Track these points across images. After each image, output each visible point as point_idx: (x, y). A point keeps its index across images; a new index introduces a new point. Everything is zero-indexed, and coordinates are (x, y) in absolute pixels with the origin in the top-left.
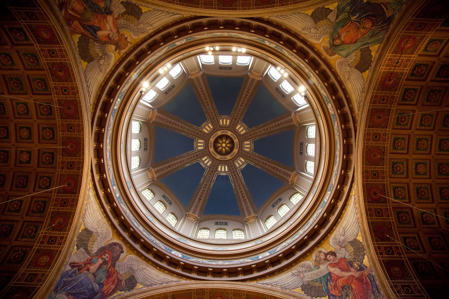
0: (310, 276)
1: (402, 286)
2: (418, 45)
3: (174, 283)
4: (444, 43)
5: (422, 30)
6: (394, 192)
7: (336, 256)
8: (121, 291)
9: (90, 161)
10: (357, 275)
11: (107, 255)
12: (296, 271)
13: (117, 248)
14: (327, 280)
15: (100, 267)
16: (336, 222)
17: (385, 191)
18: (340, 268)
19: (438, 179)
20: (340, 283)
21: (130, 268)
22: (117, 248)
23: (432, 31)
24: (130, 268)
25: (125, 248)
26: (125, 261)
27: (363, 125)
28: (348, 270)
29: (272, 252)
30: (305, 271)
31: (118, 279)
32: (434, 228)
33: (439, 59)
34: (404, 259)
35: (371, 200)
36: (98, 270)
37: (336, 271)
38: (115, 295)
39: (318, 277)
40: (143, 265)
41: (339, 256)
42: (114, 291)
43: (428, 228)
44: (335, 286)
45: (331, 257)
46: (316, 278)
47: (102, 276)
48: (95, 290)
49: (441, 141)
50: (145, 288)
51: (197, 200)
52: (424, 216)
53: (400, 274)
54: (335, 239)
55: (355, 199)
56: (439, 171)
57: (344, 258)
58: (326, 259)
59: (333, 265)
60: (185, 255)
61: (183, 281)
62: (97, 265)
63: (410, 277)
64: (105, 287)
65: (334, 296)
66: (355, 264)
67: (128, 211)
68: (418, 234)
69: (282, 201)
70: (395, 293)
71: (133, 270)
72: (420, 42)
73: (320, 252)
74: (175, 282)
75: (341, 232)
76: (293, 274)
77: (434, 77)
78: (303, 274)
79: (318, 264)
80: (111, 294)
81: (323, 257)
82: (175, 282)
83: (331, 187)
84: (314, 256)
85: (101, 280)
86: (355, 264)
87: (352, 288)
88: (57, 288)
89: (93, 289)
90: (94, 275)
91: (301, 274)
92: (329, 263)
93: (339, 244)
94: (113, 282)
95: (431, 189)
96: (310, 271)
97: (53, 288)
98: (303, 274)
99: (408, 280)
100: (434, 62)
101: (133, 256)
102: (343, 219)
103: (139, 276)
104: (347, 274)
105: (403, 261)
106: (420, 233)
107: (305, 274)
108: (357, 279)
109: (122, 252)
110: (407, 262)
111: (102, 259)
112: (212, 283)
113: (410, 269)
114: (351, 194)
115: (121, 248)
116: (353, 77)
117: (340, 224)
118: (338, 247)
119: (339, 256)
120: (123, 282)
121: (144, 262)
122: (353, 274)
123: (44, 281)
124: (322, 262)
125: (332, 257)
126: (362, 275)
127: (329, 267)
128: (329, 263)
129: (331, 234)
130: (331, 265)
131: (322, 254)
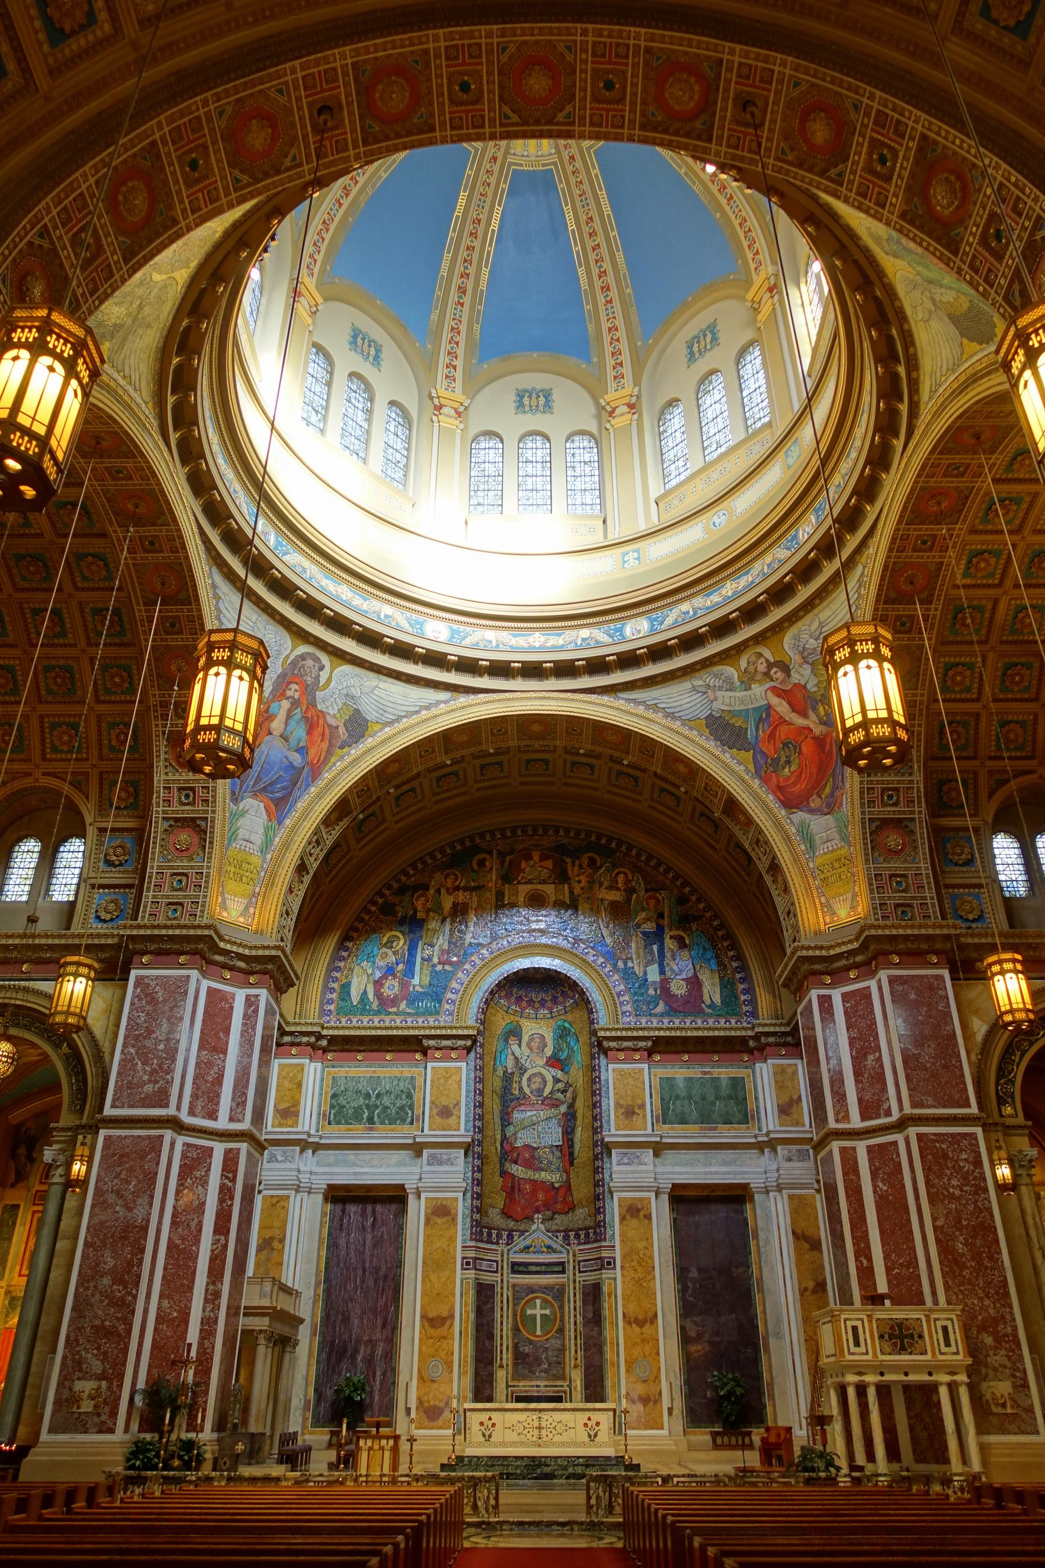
0: (727, 700)
3: (442, 706)
6: (970, 562)
7: (789, 676)
8: (342, 747)
9: (192, 518)
10: (818, 730)
11: (294, 686)
12: (701, 683)
13: (309, 662)
14: (761, 718)
15: (289, 717)
16: (809, 605)
17: (938, 576)
18: (789, 703)
20: (783, 731)
21: (347, 695)
22: (309, 662)
24: (347, 695)
25: (324, 658)
26: (332, 685)
27: (927, 445)
28: (804, 714)
29: (655, 619)
30: (720, 688)
31: (330, 726)
35: (893, 595)
36: (286, 724)
37: (782, 707)
38: (333, 759)
39: (742, 707)
40: (371, 680)
41: (795, 678)
42: (329, 752)
44: (772, 736)
45: (777, 674)
46: (738, 708)
47: (299, 733)
48: (296, 764)
50: (387, 729)
51: (454, 296)
54: (797, 638)
55: (862, 574)
57: (805, 687)
58: (767, 674)
59: (778, 692)
60: (455, 627)
61: (463, 699)
62: (282, 715)
64: (312, 752)
65: (765, 755)
66: (821, 709)
67: (306, 563)
69: (716, 349)
71: (353, 698)
73: (760, 655)
74: (445, 702)
75: (813, 629)
76: (694, 689)
78: (714, 691)
79: (748, 679)
80: (326, 760)
81: (762, 667)
82: (445, 702)
83: (820, 509)
84: (743, 664)
85: (299, 741)
86: (821, 709)
87: (800, 753)
88: (233, 793)
89: (291, 764)
90: (284, 737)
91: (710, 692)
92: (772, 684)
93: (802, 653)
94: (323, 735)
96: (731, 689)
97: (228, 797)
98: (714, 691)
99: (903, 775)
101: (347, 668)
102: (825, 603)
103: (370, 712)
104: (800, 721)
107: (719, 693)
108: (814, 738)
109: (322, 668)
111: (287, 698)
112: (521, 699)
114: (858, 558)
115: (317, 660)
116: (935, 324)
117: (816, 611)
118: (796, 658)
119: (795, 678)
120: (342, 730)
121: (371, 675)
122: (812, 726)
123: (214, 802)
124: (759, 677)
125: (780, 675)
126: (826, 736)
127: (769, 693)
128: (772, 684)
129: (791, 625)
130: (773, 689)
131: (762, 660)
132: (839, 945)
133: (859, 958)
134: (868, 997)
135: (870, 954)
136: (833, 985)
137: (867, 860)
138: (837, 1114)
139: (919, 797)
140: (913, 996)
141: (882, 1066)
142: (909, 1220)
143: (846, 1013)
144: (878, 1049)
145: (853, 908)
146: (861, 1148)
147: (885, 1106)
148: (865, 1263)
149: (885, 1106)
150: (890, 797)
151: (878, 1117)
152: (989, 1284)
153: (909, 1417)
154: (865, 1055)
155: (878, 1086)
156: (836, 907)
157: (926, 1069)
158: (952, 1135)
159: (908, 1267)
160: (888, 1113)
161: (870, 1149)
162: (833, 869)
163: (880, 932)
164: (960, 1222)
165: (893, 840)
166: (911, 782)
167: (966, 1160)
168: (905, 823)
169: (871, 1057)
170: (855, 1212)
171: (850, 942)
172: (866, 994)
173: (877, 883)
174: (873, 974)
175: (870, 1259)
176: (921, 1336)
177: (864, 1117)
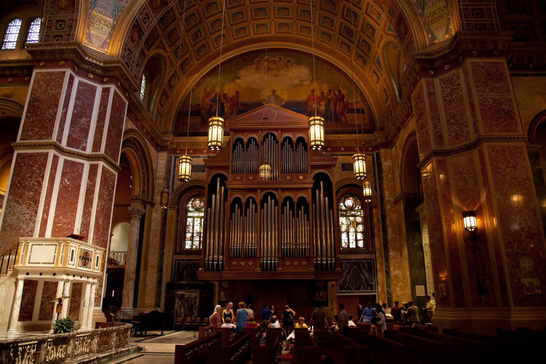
1: (147, 14)
2: (378, 4)
4: (377, 20)
5: (389, 12)
19: (251, 9)
23: (386, 19)
32: (205, 14)
33: (363, 14)
34: (170, 4)
43: (203, 10)
49: (288, 9)
52: (214, 5)
53: (156, 6)
56: (259, 9)
63: (157, 15)
68: (195, 4)
70: (139, 11)
72: (380, 7)
77: (348, 7)
95: (241, 6)
99: (153, 15)
100: (361, 9)
105: (168, 4)
106: (197, 6)
110: (168, 7)
113: (163, 12)
132: (93, 59)
133: (99, 71)
134: (95, 91)
135: (109, 74)
136: (77, 74)
137: (127, 34)
138: (58, 136)
139: (151, 28)
140: (117, 105)
141: (89, 126)
142: (77, 203)
143: (78, 91)
144: (90, 117)
145: (102, 47)
146: (62, 159)
147: (84, 145)
148: (45, 216)
149: (84, 145)
150: (145, 18)
151: (77, 148)
152: (103, 240)
153: (43, 297)
154: (81, 117)
155: (83, 134)
156: (93, 40)
157: (112, 139)
158: (111, 172)
159: (68, 224)
160: (84, 149)
161: (66, 162)
162: (100, 22)
163: (123, 69)
164: (103, 211)
165: (136, 35)
166: (153, 20)
167: (111, 185)
168: (141, 33)
169: (84, 119)
170: (49, 190)
171: (101, 62)
172: (93, 90)
173: (126, 48)
174: (102, 82)
175: (47, 215)
176: (91, 260)
177: (68, 145)
